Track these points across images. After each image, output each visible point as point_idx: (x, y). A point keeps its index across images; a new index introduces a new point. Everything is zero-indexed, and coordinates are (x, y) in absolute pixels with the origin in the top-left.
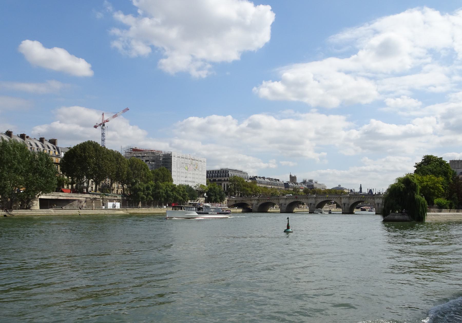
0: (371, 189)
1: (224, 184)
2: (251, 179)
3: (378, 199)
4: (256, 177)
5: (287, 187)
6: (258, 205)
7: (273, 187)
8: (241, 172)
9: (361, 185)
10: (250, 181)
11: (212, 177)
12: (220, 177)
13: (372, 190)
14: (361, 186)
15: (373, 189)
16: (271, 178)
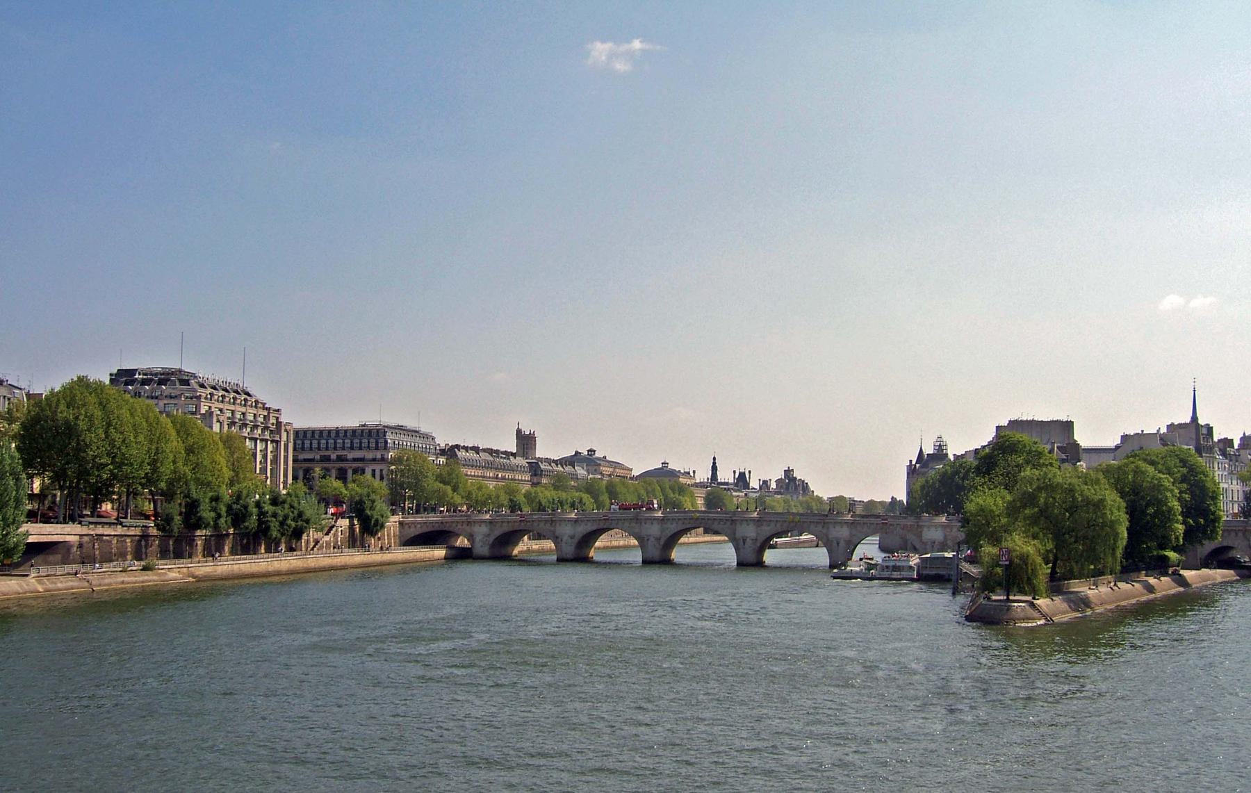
0: (742, 470)
1: (374, 471)
2: (443, 452)
3: (838, 528)
4: (457, 446)
5: (536, 475)
6: (492, 539)
7: (500, 476)
8: (415, 432)
9: (714, 459)
10: (442, 460)
11: (319, 449)
12: (360, 448)
13: (747, 476)
14: (714, 463)
15: (750, 472)
16: (495, 448)
